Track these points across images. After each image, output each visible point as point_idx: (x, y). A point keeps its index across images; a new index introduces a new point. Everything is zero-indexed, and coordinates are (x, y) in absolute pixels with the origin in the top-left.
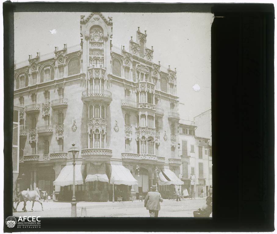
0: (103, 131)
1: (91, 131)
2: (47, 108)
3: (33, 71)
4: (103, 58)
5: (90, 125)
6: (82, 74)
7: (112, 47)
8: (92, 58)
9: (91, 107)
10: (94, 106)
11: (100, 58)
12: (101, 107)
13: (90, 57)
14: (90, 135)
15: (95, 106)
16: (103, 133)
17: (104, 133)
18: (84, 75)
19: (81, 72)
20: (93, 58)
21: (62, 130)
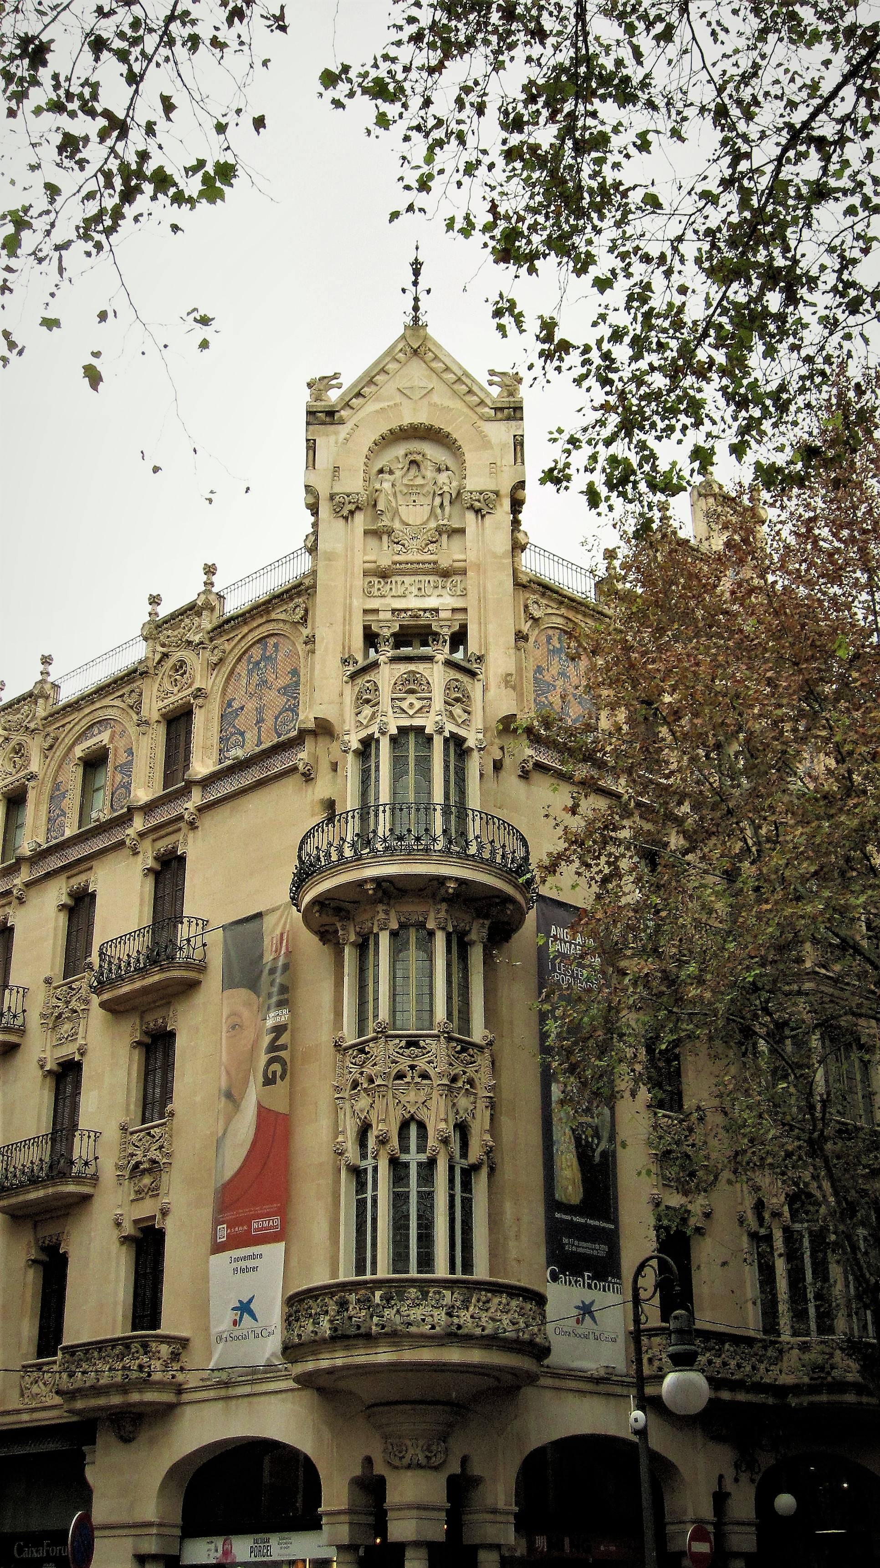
0: (462, 1128)
1: (364, 1130)
2: (74, 1004)
3: (10, 779)
4: (465, 610)
5: (355, 1085)
6: (313, 733)
7: (523, 548)
8: (382, 616)
9: (364, 946)
10: (384, 940)
11: (442, 615)
12: (440, 940)
13: (366, 612)
14: (358, 1173)
15: (394, 934)
16: (464, 1154)
17: (475, 1153)
18: (324, 729)
19: (307, 717)
20: (388, 616)
21: (154, 1154)
